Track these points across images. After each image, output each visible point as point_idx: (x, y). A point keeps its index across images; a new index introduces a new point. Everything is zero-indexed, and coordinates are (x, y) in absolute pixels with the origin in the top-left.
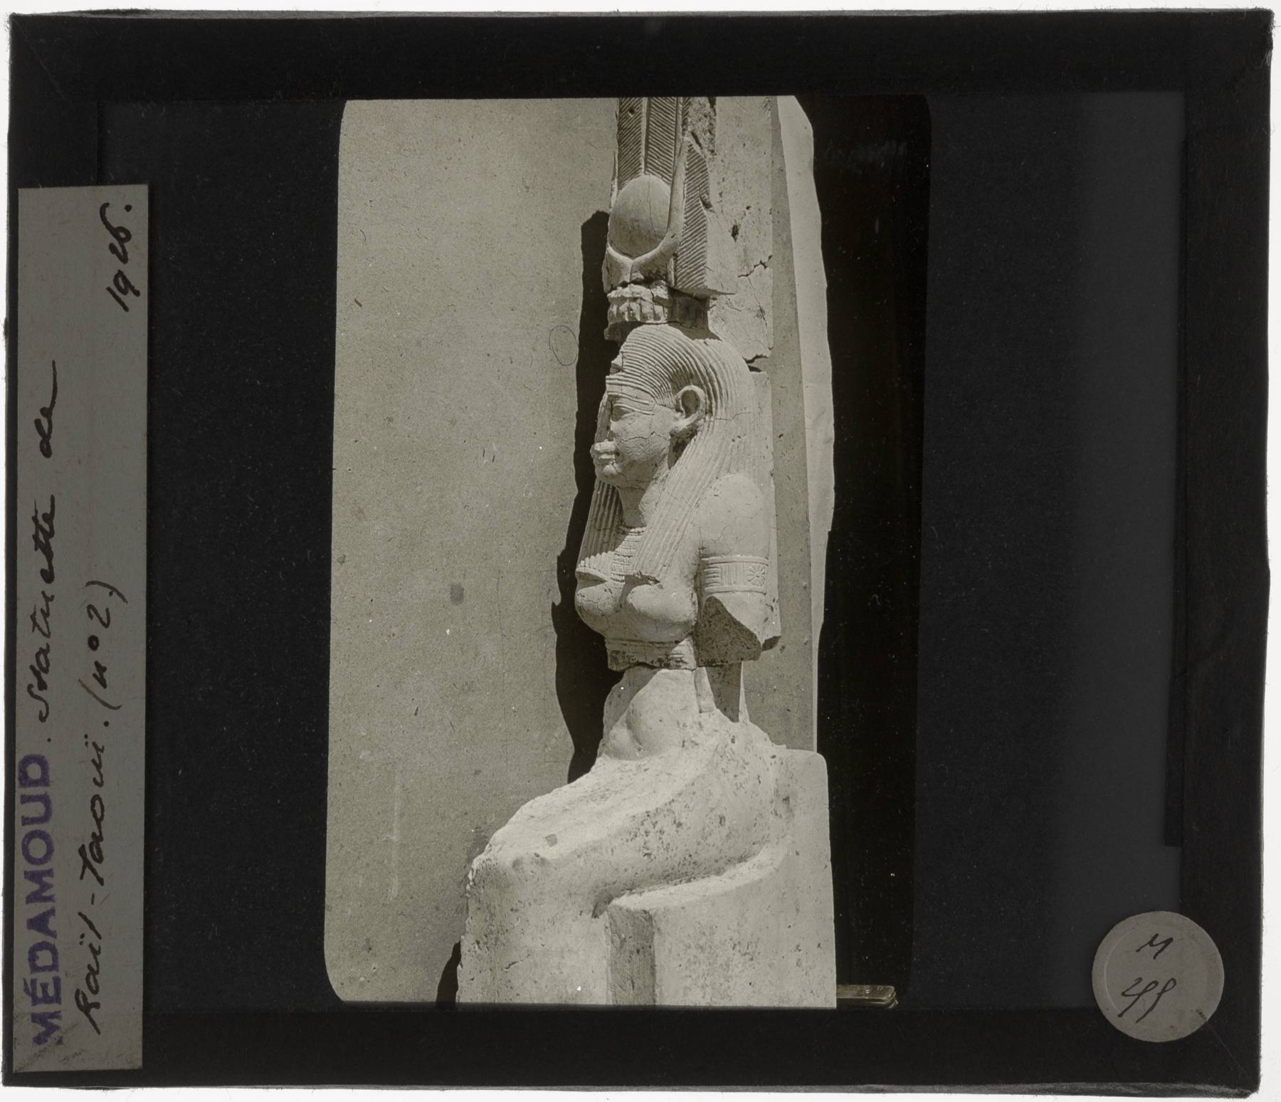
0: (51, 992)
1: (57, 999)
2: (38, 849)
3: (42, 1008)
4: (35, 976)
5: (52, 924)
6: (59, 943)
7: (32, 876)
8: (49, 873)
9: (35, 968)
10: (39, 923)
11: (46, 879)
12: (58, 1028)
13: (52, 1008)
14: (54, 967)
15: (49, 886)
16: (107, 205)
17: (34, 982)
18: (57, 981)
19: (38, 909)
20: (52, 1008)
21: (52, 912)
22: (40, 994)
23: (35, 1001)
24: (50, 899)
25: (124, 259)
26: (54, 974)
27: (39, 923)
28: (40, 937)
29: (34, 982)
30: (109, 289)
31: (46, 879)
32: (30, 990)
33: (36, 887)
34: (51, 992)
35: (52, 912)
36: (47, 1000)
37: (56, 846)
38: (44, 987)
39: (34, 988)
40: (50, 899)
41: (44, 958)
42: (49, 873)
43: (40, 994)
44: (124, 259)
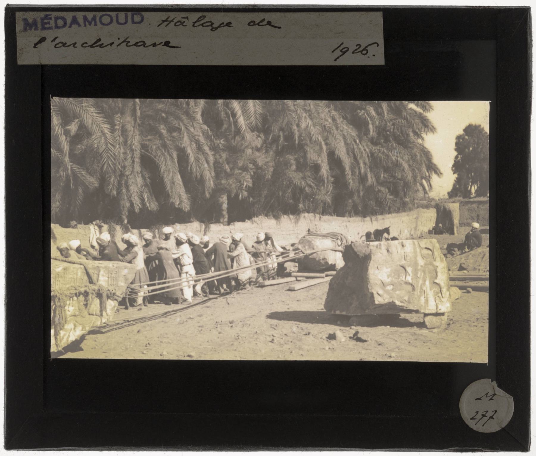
0: (47, 26)
1: (44, 28)
2: (106, 19)
4: (53, 19)
5: (74, 26)
6: (67, 28)
8: (96, 25)
9: (57, 18)
10: (74, 21)
12: (31, 29)
13: (39, 26)
14: (57, 27)
15: (90, 24)
17: (51, 19)
19: (81, 20)
20: (39, 26)
21: (79, 25)
22: (46, 21)
23: (42, 19)
24: (85, 25)
26: (54, 27)
27: (74, 21)
28: (69, 21)
29: (51, 19)
31: (93, 23)
32: (46, 17)
35: (79, 25)
36: (43, 24)
38: (49, 23)
39: (47, 19)
40: (85, 25)
41: (60, 22)
42: (96, 25)
43: (46, 21)
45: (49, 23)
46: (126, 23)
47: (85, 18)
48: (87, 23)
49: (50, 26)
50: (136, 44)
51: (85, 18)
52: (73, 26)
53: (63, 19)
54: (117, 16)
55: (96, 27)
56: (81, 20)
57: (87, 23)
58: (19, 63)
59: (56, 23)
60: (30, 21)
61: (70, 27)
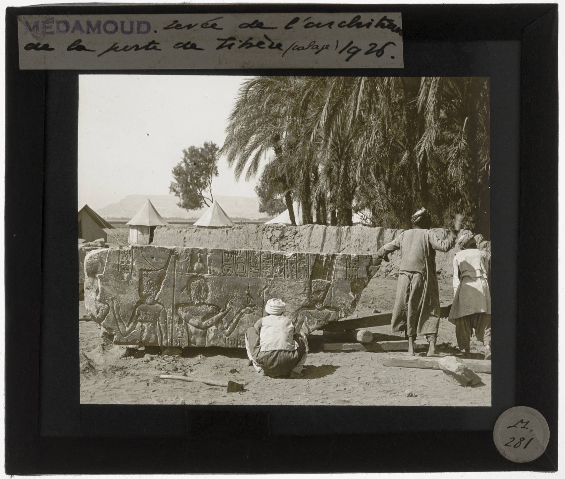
0: (47, 30)
1: (45, 33)
2: (110, 27)
3: (40, 24)
5: (77, 32)
7: (98, 24)
9: (59, 22)
11: (97, 30)
13: (41, 30)
15: (94, 30)
16: (394, 44)
18: (52, 33)
21: (83, 31)
22: (47, 25)
25: (367, 53)
30: (352, 43)
31: (97, 30)
33: (94, 26)
34: (47, 30)
37: (107, 35)
40: (88, 32)
41: (63, 27)
42: (99, 32)
43: (47, 25)
44: (367, 53)
45: (51, 27)
46: (131, 31)
47: (89, 24)
48: (91, 31)
49: (52, 30)
50: (125, 49)
51: (89, 24)
52: (76, 31)
53: (66, 23)
54: (123, 23)
55: (99, 35)
56: (85, 27)
57: (91, 31)
58: (22, 67)
59: (58, 28)
60: (32, 26)
61: (73, 32)
